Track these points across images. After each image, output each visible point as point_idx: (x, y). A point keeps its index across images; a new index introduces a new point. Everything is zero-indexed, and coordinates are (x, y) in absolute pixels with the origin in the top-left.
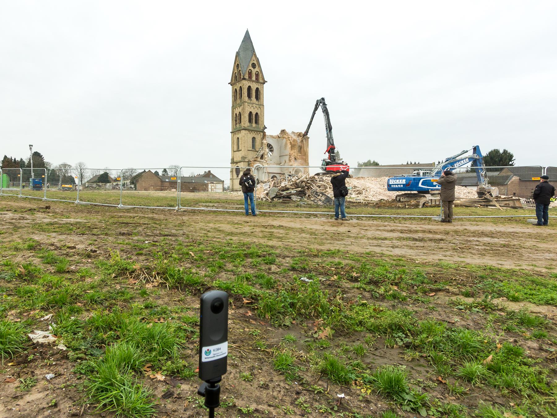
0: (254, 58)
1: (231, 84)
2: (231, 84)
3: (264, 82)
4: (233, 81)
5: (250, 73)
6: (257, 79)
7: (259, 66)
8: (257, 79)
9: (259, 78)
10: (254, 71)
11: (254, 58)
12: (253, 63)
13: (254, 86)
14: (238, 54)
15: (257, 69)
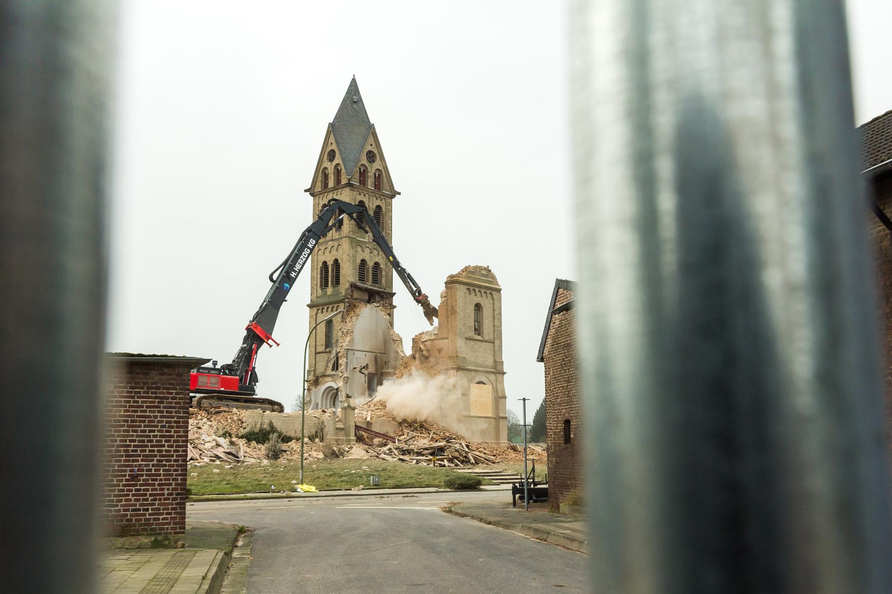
0: (371, 140)
1: (311, 191)
2: (311, 191)
3: (394, 194)
4: (318, 188)
5: (363, 174)
6: (378, 185)
7: (382, 159)
8: (378, 185)
9: (383, 186)
10: (372, 169)
11: (371, 140)
12: (370, 152)
14: (332, 128)
15: (377, 165)
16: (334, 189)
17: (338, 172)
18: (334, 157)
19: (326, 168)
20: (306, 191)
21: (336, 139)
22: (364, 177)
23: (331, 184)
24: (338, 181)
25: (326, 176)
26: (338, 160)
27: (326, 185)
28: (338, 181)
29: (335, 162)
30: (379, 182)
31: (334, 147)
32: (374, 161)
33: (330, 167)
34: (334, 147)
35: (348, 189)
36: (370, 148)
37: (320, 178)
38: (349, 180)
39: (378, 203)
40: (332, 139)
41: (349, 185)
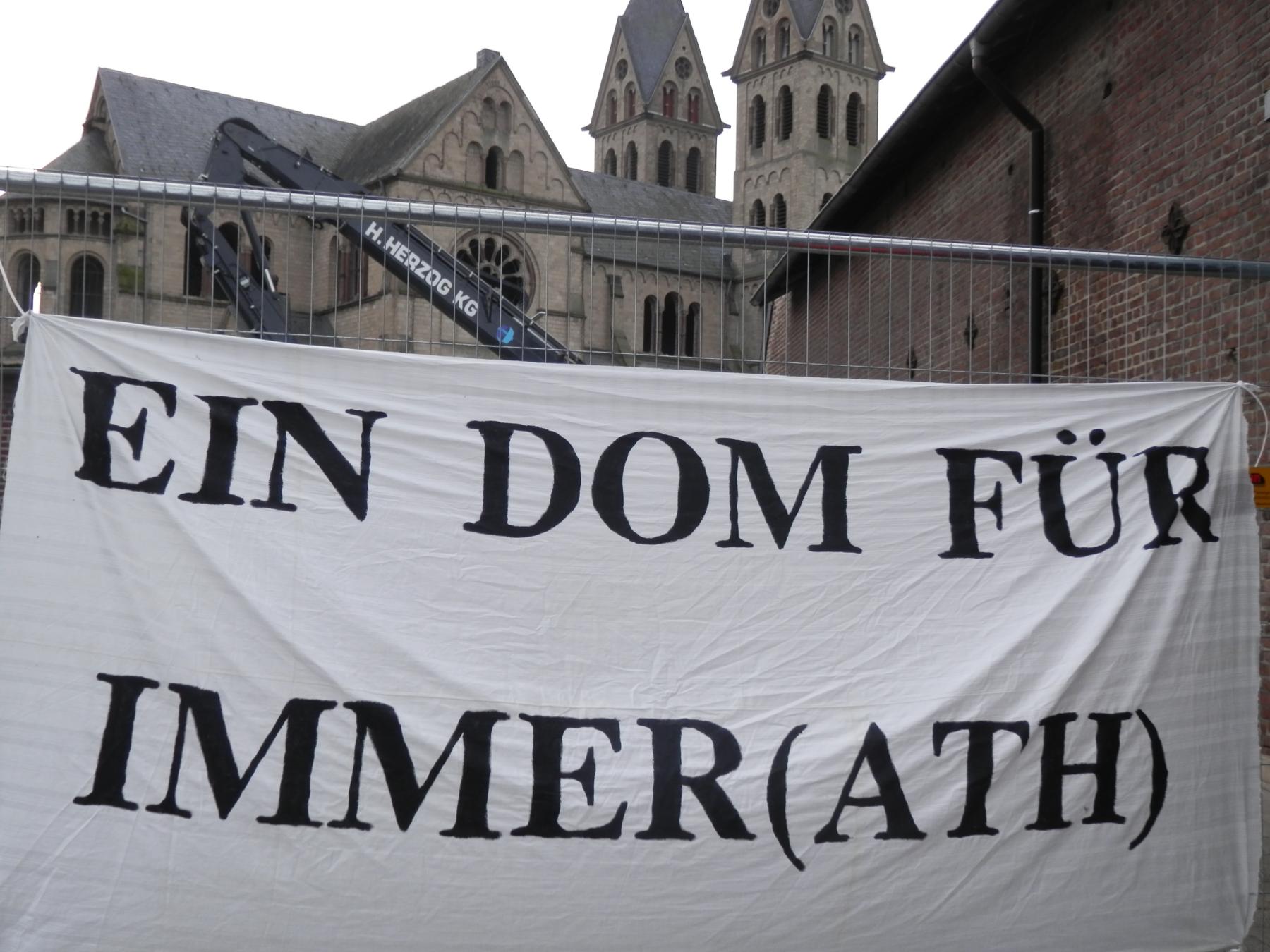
0: (683, 39)
1: (592, 129)
4: (602, 125)
5: (669, 98)
11: (683, 39)
12: (682, 60)
13: (682, 146)
14: (624, 25)
15: (693, 81)
16: (625, 124)
17: (631, 96)
18: (625, 71)
19: (613, 91)
20: (584, 129)
21: (628, 41)
22: (672, 103)
23: (620, 117)
24: (631, 111)
25: (614, 104)
26: (630, 77)
27: (613, 117)
28: (631, 111)
29: (628, 79)
30: (696, 109)
31: (625, 55)
32: (687, 75)
33: (619, 87)
34: (625, 55)
35: (644, 123)
36: (682, 54)
37: (605, 107)
38: (646, 108)
39: (693, 143)
40: (623, 43)
41: (647, 116)
